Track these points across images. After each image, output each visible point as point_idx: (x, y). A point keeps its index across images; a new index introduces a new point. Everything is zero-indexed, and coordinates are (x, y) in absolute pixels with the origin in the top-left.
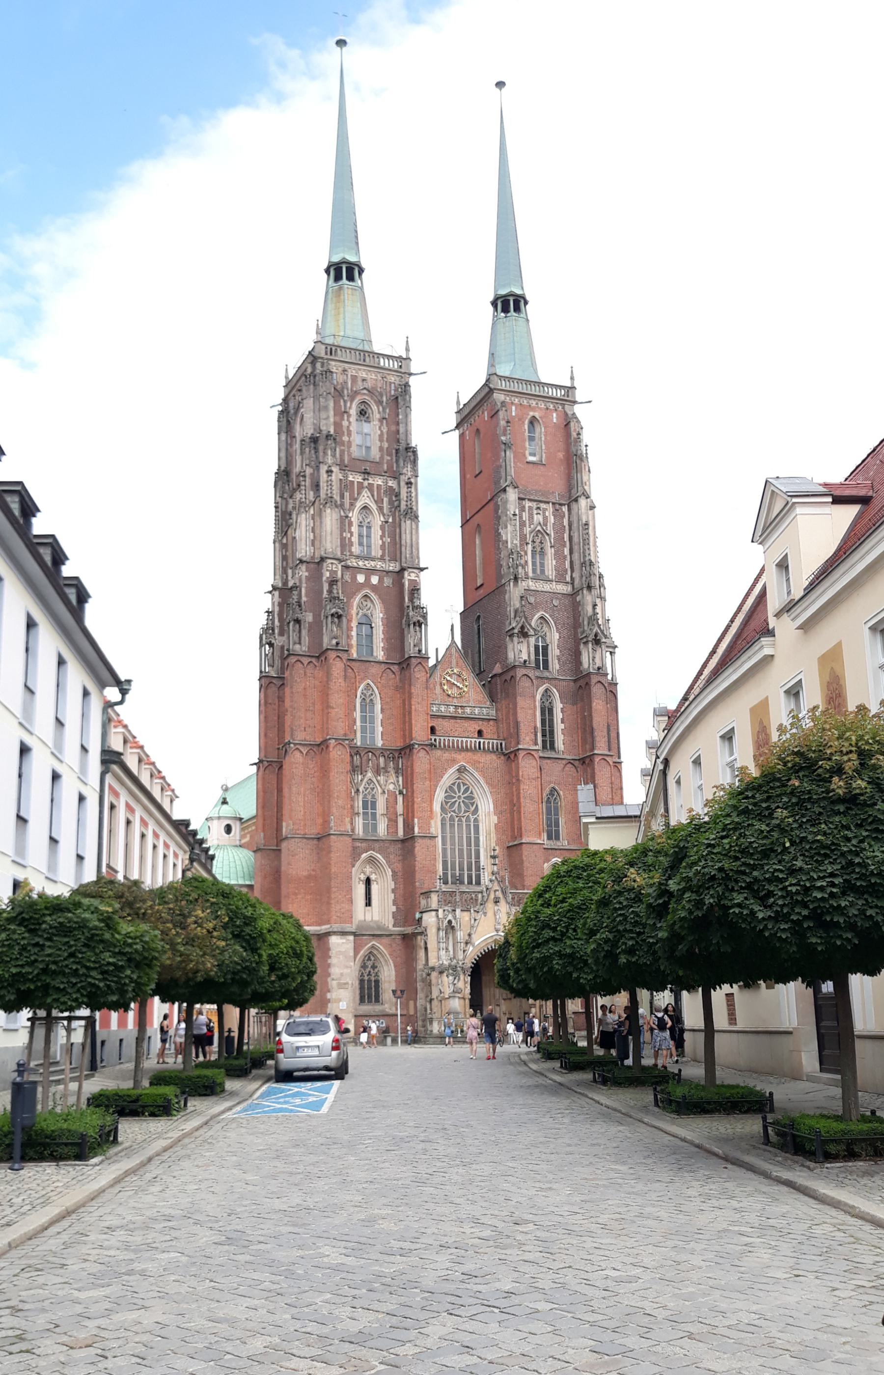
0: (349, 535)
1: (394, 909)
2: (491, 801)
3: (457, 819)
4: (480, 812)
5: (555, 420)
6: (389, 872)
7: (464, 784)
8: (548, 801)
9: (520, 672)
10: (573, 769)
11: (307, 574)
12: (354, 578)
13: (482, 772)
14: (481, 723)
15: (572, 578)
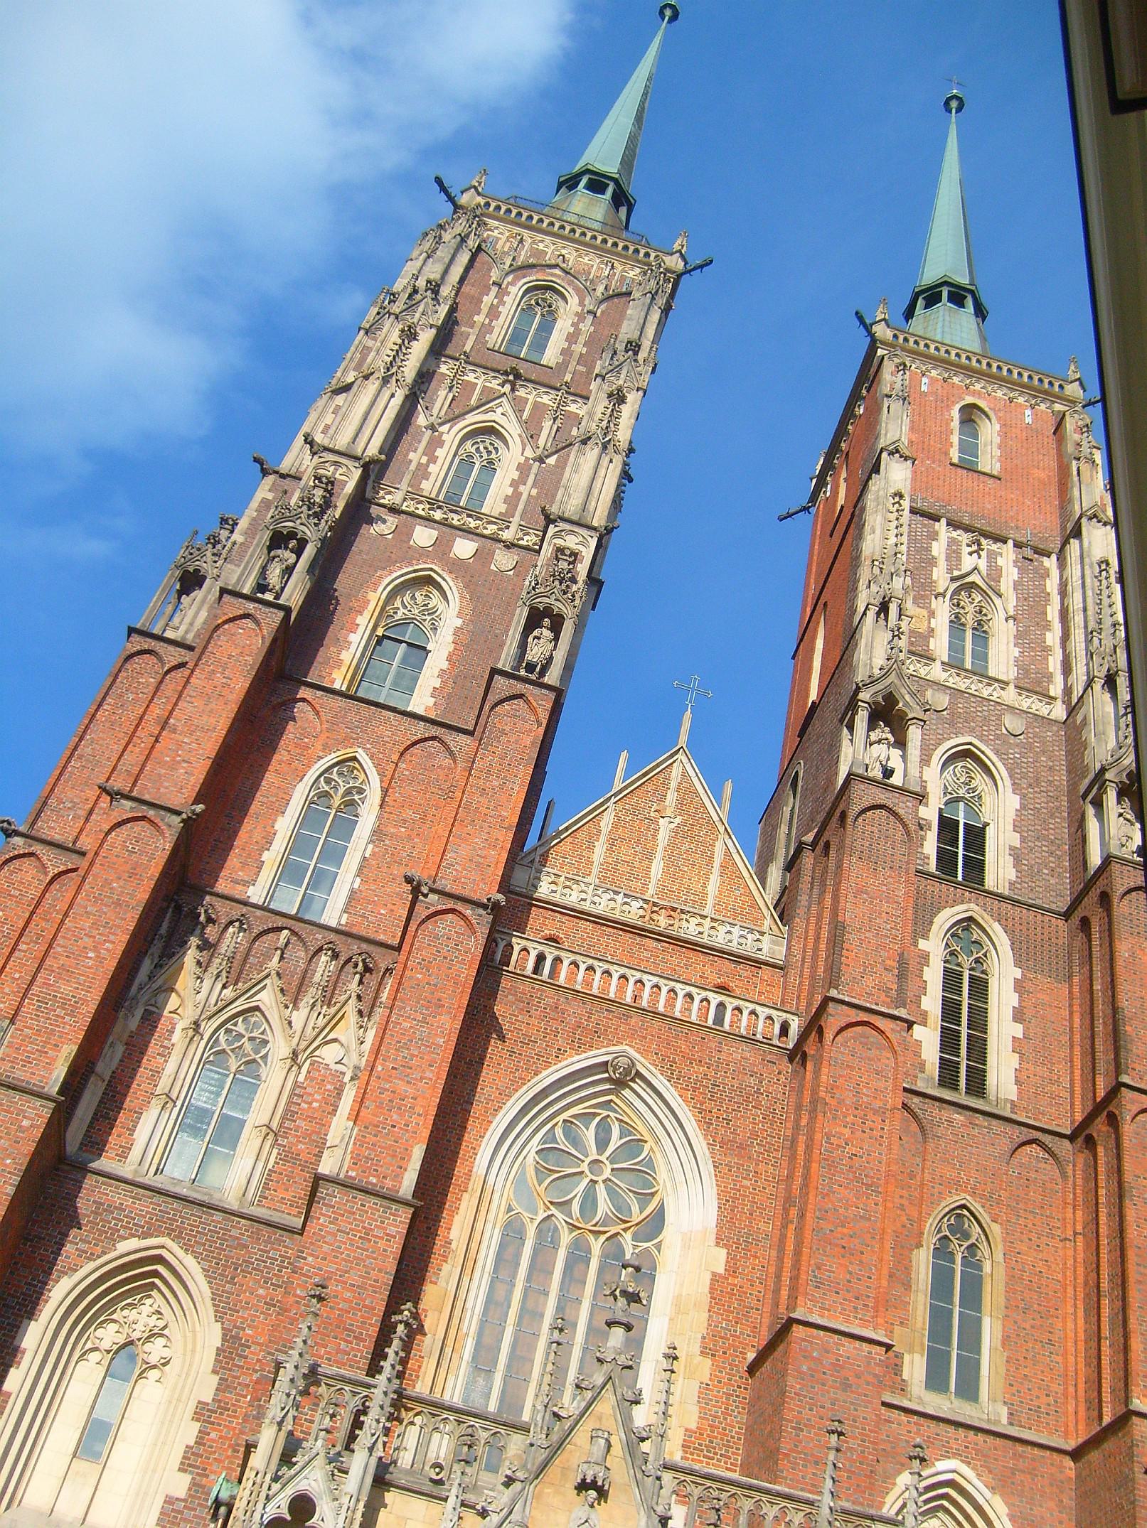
0: (424, 460)
1: (180, 1485)
2: (712, 1191)
3: (566, 1237)
4: (669, 1234)
5: (1028, 420)
6: (213, 1336)
7: (626, 1129)
8: (942, 1251)
9: (862, 796)
10: (1050, 1168)
11: (270, 496)
12: (403, 534)
13: (691, 1090)
14: (727, 966)
15: (1067, 691)
